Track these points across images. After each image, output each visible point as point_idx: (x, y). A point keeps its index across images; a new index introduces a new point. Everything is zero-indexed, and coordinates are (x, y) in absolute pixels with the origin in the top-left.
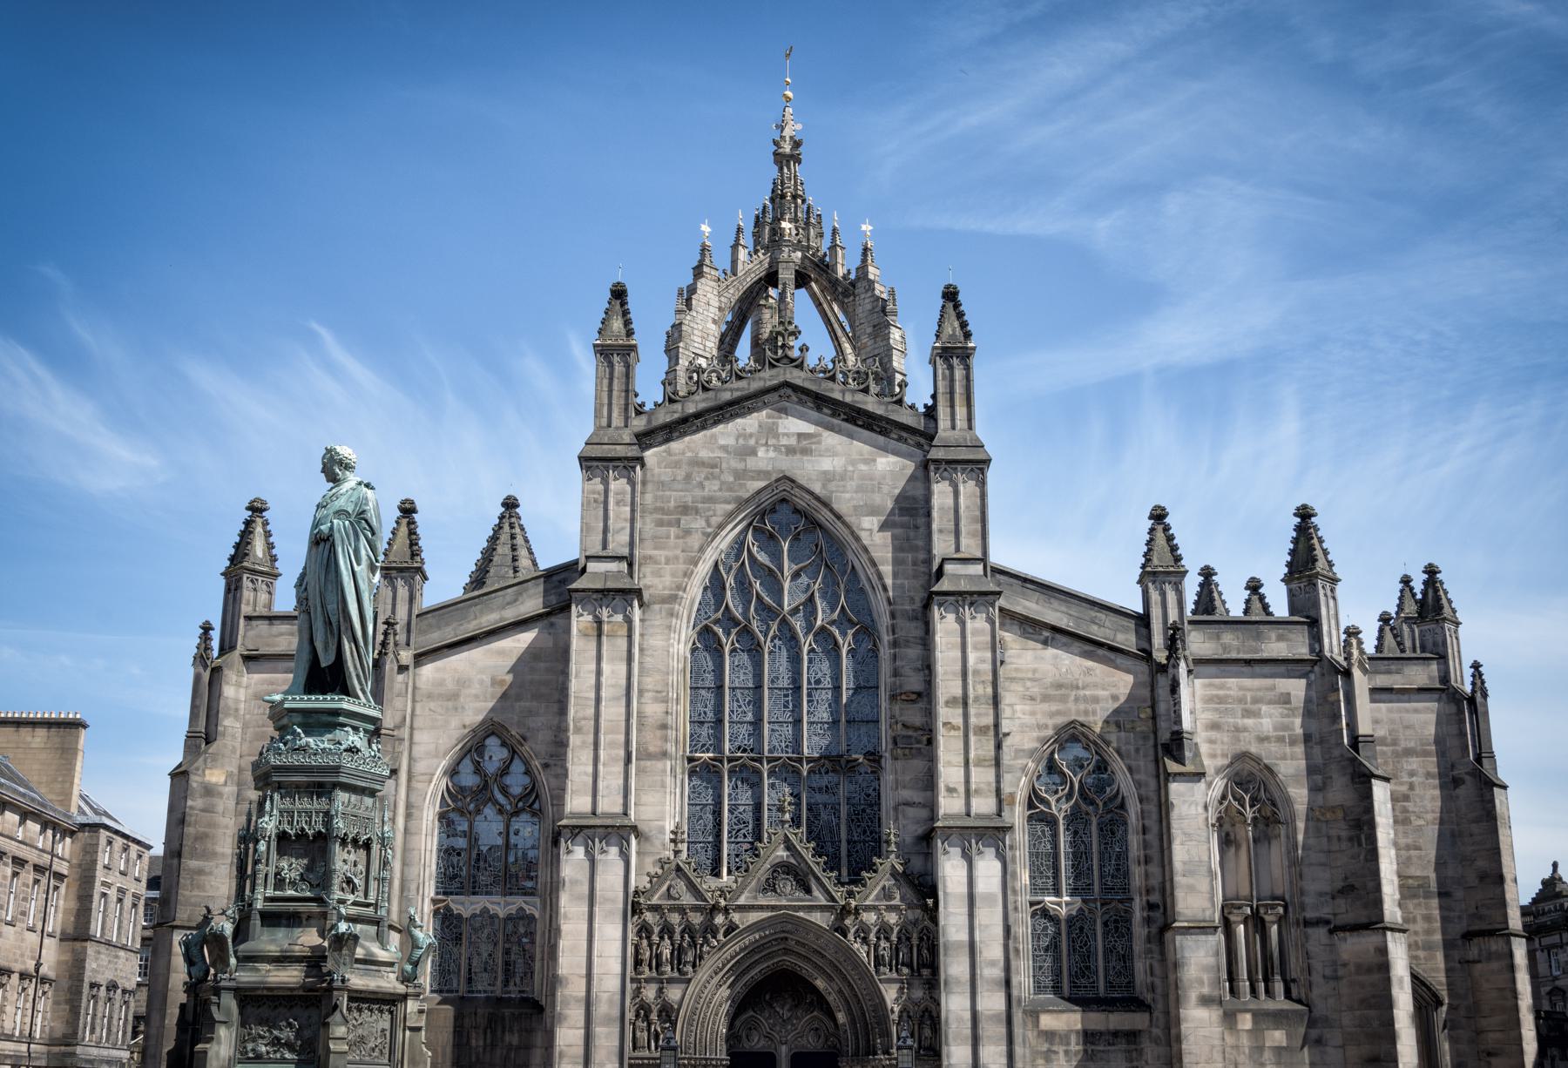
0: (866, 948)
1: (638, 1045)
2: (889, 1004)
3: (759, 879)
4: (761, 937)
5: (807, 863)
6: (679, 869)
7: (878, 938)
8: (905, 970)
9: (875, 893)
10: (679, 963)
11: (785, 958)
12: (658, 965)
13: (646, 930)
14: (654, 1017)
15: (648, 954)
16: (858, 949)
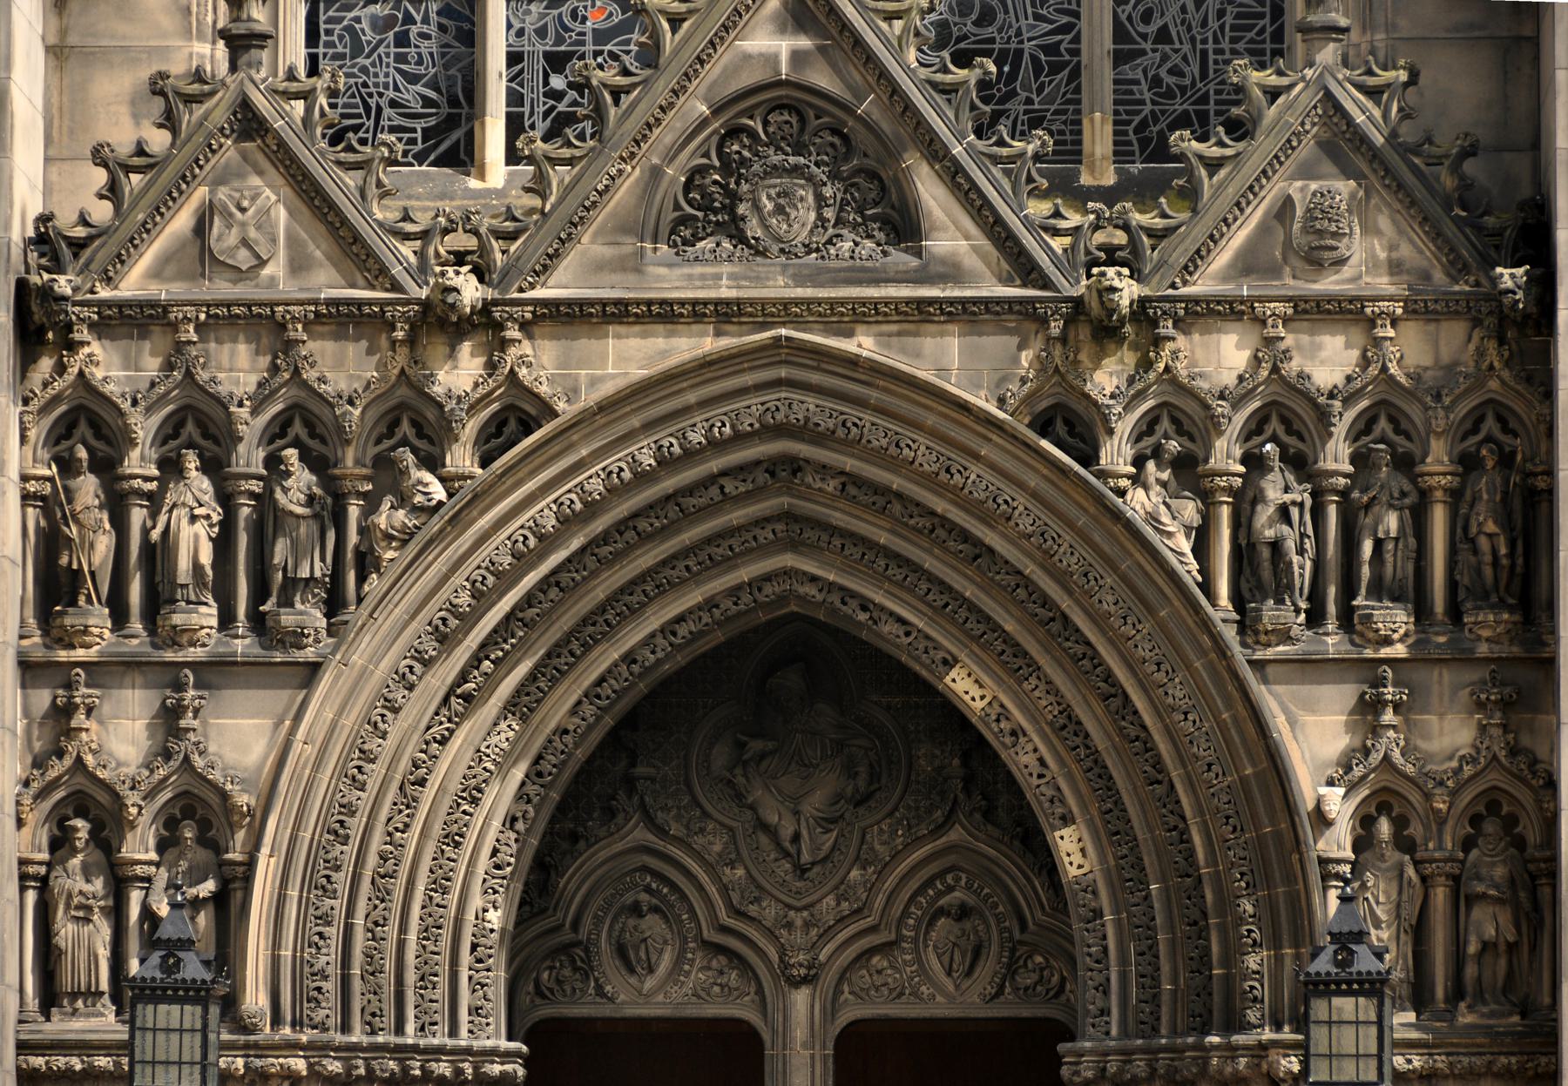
0: (1190, 510)
1: (66, 982)
2: (1308, 786)
3: (655, 173)
4: (666, 463)
5: (895, 90)
6: (248, 123)
7: (1254, 463)
8: (1395, 619)
9: (1239, 238)
10: (260, 591)
11: (788, 560)
12: (158, 600)
13: (97, 426)
14: (139, 847)
15: (104, 544)
16: (1153, 518)
